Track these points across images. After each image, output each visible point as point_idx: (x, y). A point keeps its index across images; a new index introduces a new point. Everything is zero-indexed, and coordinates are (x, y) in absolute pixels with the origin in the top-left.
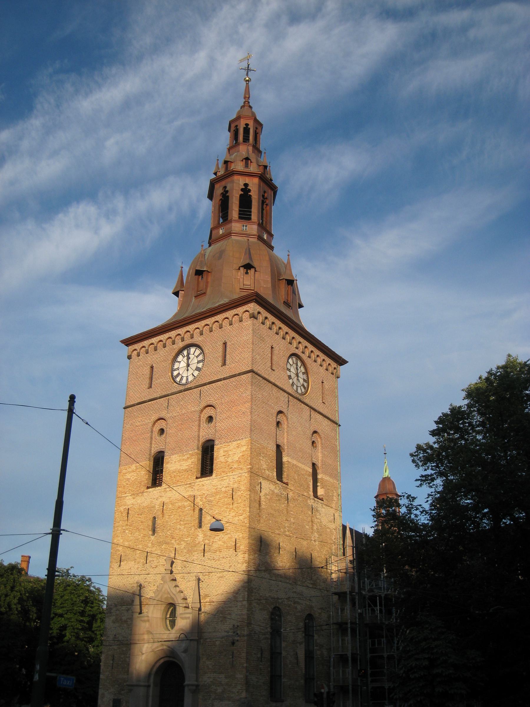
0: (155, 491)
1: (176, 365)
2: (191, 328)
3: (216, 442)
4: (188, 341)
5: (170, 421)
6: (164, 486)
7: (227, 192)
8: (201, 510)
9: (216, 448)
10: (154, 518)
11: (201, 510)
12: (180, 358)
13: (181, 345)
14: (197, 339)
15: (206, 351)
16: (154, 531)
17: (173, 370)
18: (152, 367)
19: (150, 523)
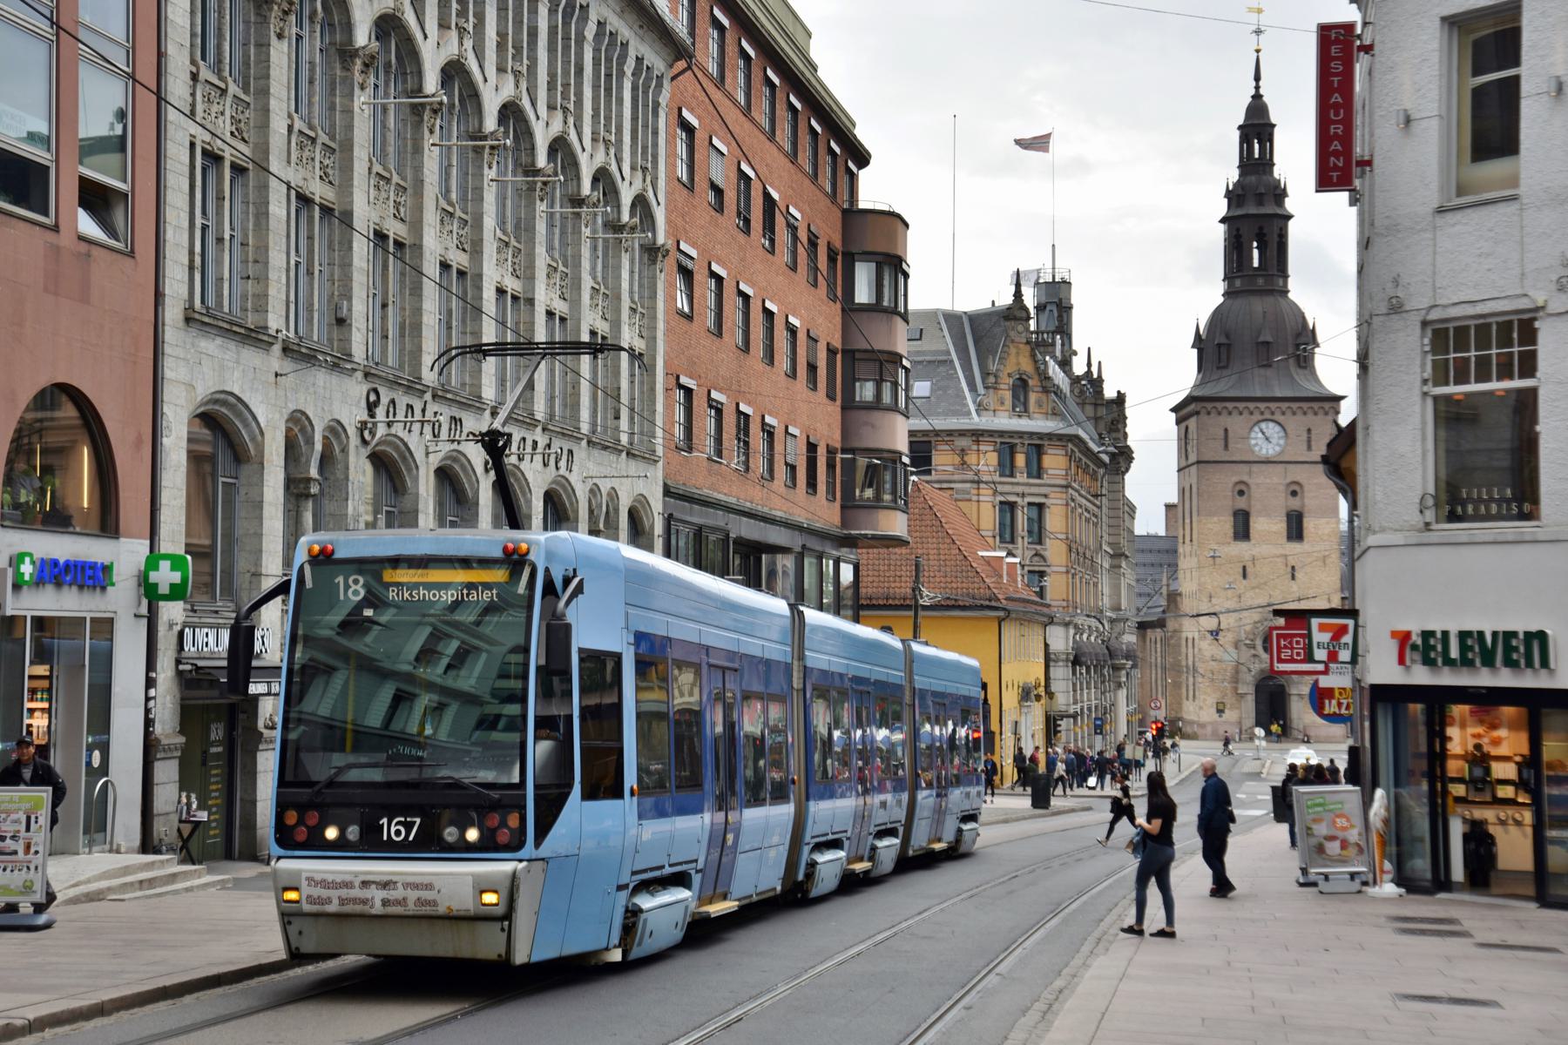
0: (1243, 546)
1: (1253, 435)
2: (1273, 405)
3: (1306, 515)
4: (1268, 416)
5: (1253, 487)
6: (1253, 542)
7: (1265, 235)
8: (1293, 568)
9: (1305, 521)
10: (1244, 568)
11: (1293, 568)
12: (1256, 429)
13: (1260, 418)
14: (1278, 417)
15: (1289, 430)
16: (1245, 576)
17: (1248, 438)
18: (1226, 430)
19: (1241, 570)
